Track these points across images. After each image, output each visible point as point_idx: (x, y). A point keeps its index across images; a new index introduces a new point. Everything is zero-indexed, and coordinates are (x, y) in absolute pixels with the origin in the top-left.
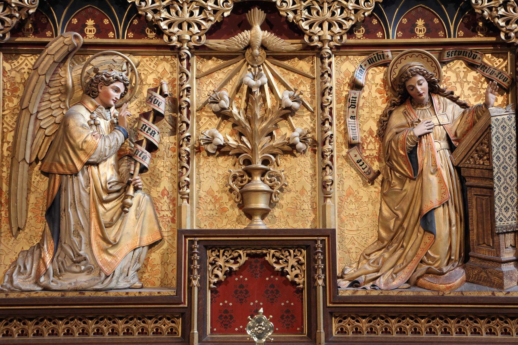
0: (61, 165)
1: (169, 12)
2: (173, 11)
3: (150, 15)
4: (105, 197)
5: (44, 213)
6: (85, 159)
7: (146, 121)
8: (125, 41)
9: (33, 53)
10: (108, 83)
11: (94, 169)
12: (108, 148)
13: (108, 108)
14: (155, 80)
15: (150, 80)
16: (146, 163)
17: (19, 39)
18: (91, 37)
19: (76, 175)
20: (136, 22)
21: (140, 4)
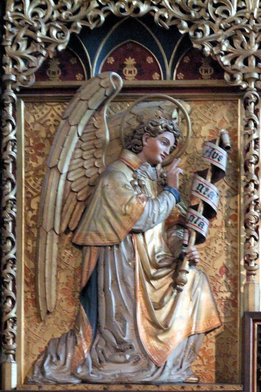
0: (99, 235)
1: (232, 43)
2: (237, 43)
3: (207, 49)
4: (153, 271)
5: (77, 295)
6: (129, 226)
7: (202, 179)
8: (174, 82)
9: (62, 101)
10: (154, 133)
11: (140, 237)
12: (156, 213)
13: (154, 165)
14: (211, 132)
15: (205, 131)
16: (204, 232)
17: (44, 84)
18: (131, 79)
19: (118, 246)
20: (187, 60)
21: (195, 35)
